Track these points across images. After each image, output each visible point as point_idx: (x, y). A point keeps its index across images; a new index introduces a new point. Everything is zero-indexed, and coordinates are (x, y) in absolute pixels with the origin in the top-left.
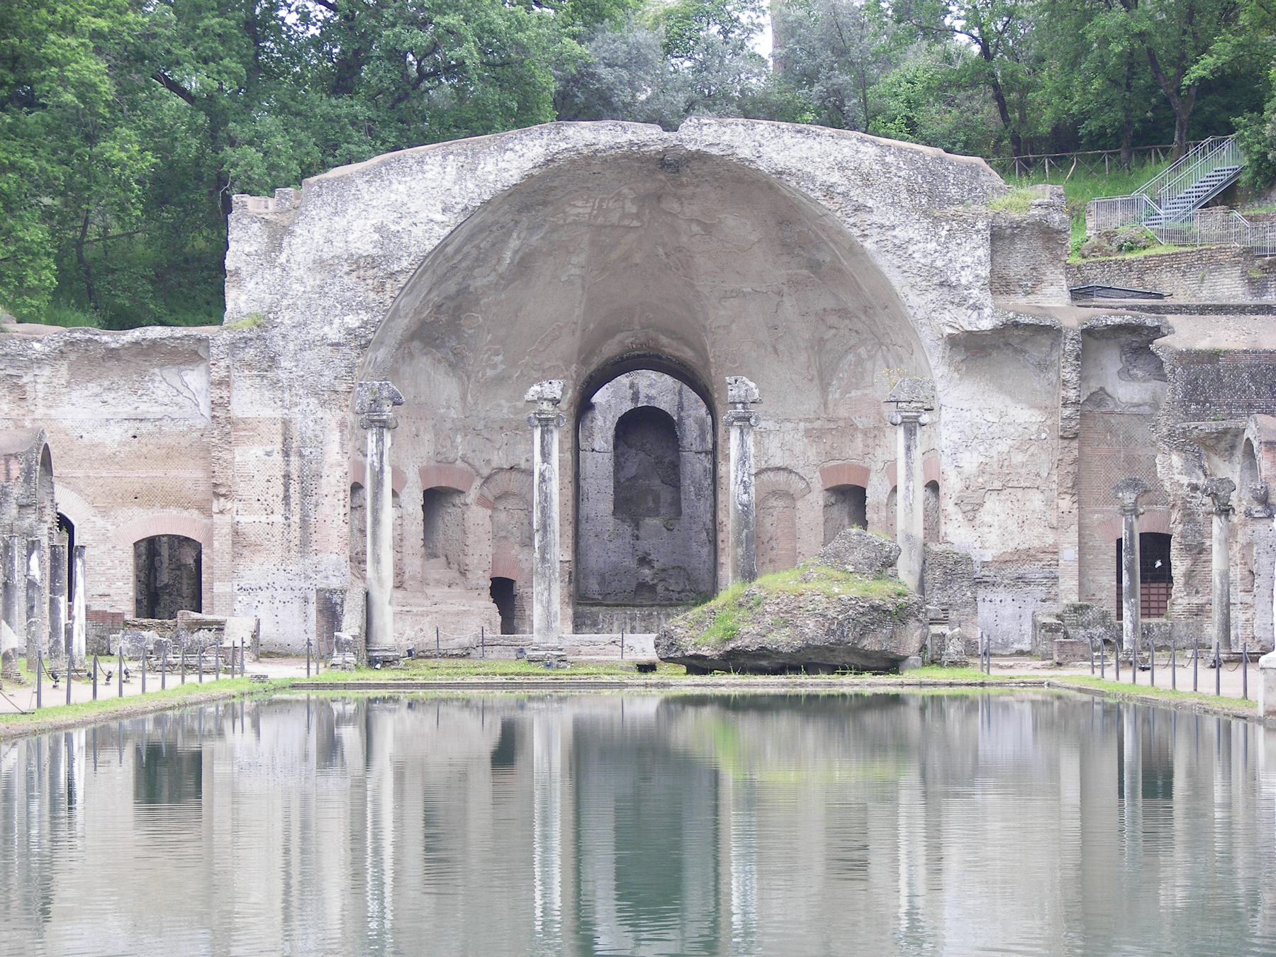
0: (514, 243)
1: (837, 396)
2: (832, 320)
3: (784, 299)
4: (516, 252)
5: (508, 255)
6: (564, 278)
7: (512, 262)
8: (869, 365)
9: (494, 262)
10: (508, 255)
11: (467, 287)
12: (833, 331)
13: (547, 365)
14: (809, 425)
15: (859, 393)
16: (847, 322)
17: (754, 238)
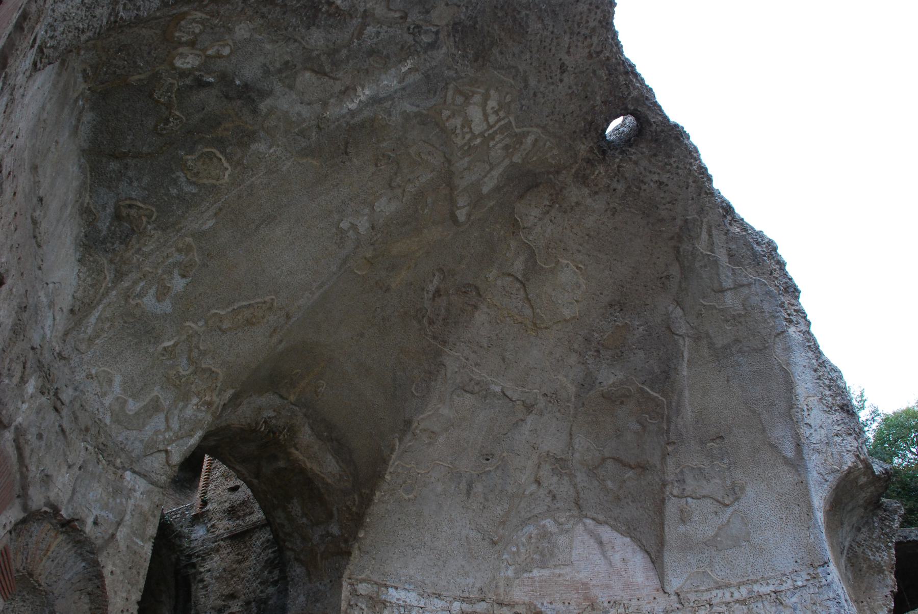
0: (389, 81)
1: (510, 573)
2: (545, 472)
3: (530, 419)
4: (375, 100)
5: (365, 93)
6: (344, 225)
7: (352, 113)
8: (562, 540)
9: (338, 87)
10: (365, 93)
11: (264, 94)
12: (534, 487)
13: (207, 363)
14: (466, 607)
15: (546, 573)
16: (555, 479)
17: (567, 313)
